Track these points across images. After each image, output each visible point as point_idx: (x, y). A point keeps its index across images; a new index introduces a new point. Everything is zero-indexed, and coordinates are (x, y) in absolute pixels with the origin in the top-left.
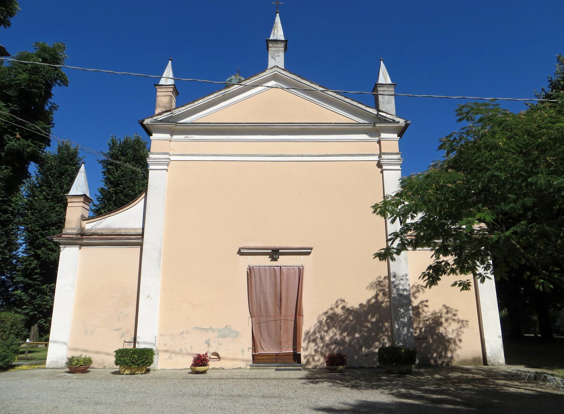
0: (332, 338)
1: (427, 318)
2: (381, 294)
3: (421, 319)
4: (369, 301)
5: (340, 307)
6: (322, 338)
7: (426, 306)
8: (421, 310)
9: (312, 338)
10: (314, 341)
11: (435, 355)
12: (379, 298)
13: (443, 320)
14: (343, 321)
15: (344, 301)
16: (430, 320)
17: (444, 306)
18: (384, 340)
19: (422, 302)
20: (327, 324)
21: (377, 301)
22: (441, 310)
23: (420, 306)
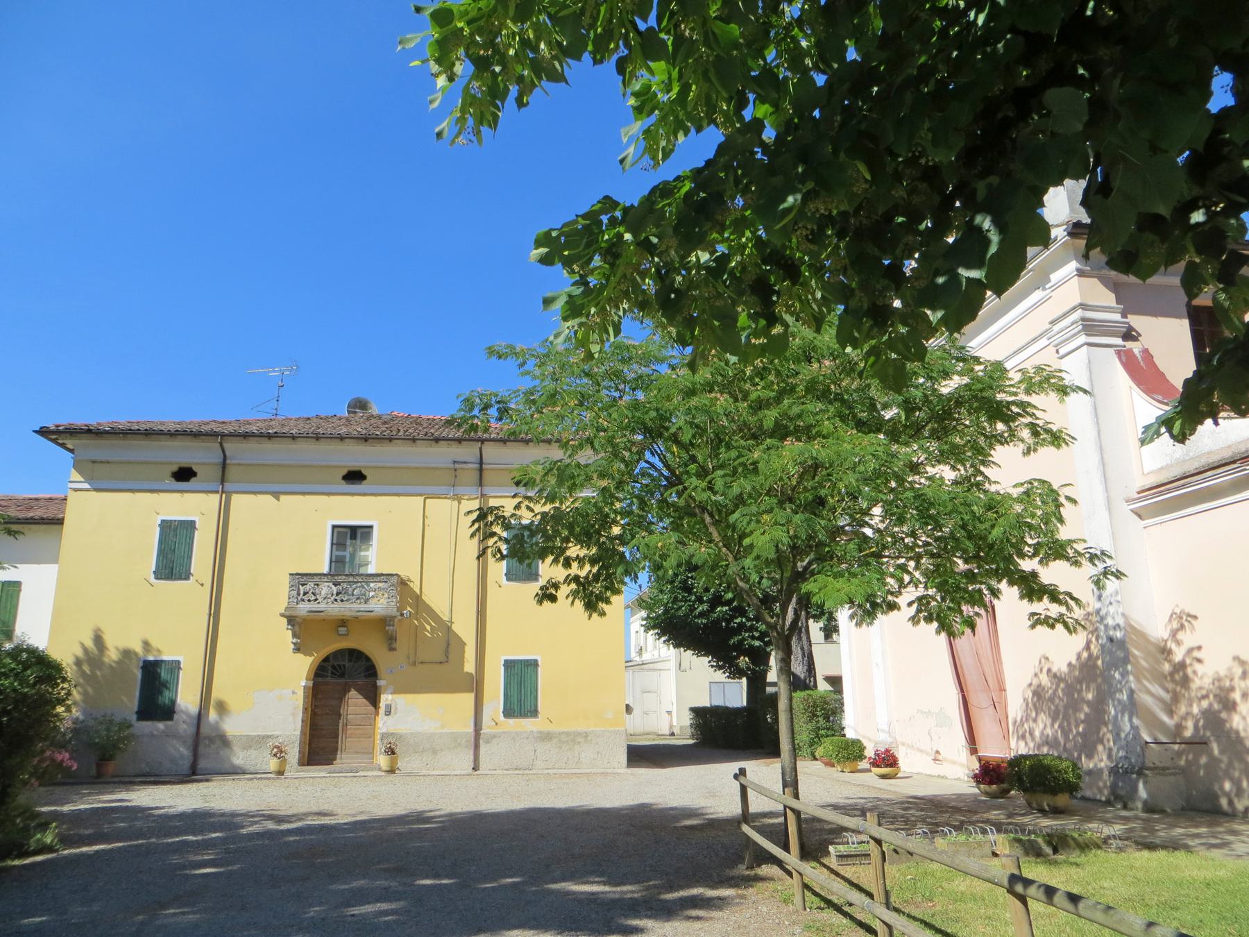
0: (1042, 733)
1: (1204, 692)
2: (1094, 639)
3: (1193, 694)
4: (1079, 656)
5: (1045, 670)
6: (1031, 734)
7: (1199, 661)
8: (1189, 671)
9: (1020, 733)
10: (1023, 737)
11: (1227, 786)
12: (1092, 647)
13: (1237, 696)
14: (1051, 700)
15: (1047, 659)
16: (1211, 697)
17: (1236, 658)
18: (1108, 741)
19: (1190, 651)
20: (1034, 705)
21: (1090, 656)
22: (1230, 669)
23: (1188, 661)
